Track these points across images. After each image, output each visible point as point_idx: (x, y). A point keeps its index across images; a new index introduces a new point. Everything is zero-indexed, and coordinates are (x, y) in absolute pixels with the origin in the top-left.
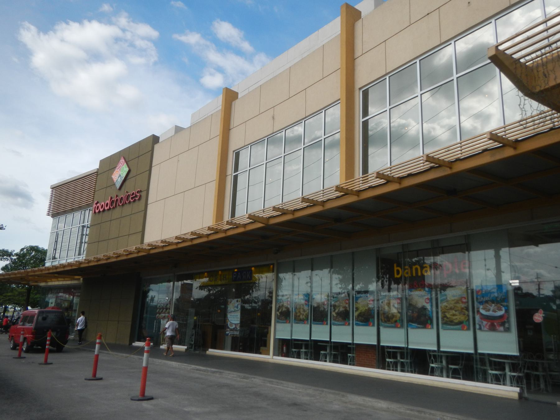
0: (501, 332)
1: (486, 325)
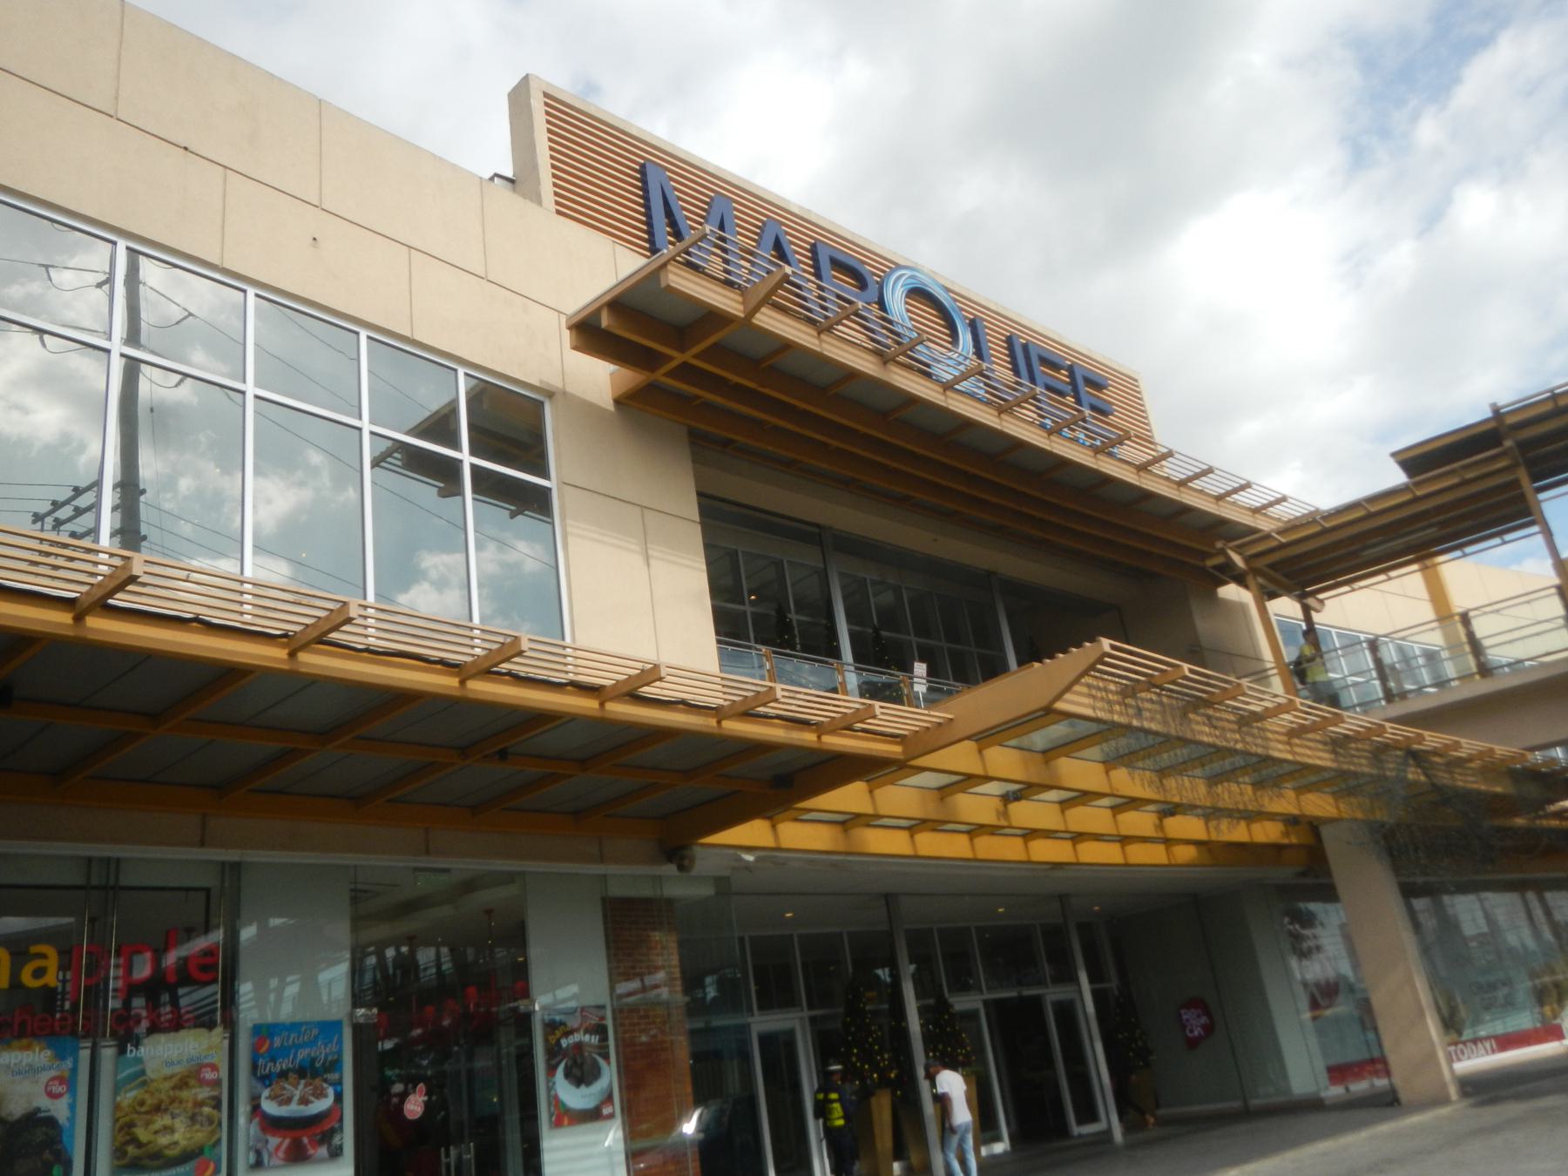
0: (321, 1161)
1: (277, 1148)
